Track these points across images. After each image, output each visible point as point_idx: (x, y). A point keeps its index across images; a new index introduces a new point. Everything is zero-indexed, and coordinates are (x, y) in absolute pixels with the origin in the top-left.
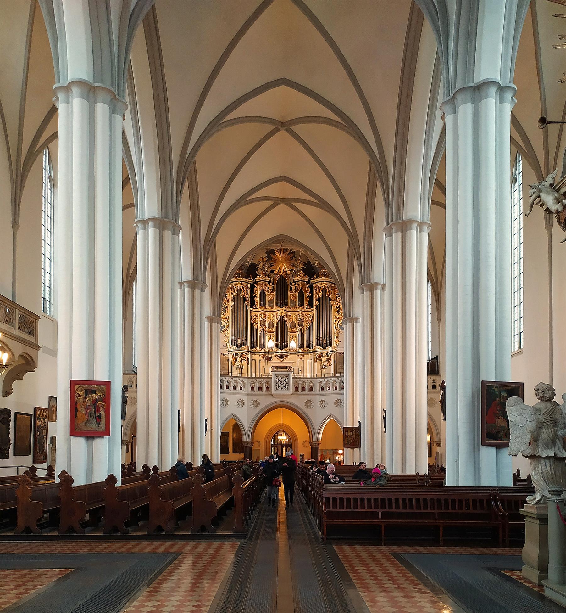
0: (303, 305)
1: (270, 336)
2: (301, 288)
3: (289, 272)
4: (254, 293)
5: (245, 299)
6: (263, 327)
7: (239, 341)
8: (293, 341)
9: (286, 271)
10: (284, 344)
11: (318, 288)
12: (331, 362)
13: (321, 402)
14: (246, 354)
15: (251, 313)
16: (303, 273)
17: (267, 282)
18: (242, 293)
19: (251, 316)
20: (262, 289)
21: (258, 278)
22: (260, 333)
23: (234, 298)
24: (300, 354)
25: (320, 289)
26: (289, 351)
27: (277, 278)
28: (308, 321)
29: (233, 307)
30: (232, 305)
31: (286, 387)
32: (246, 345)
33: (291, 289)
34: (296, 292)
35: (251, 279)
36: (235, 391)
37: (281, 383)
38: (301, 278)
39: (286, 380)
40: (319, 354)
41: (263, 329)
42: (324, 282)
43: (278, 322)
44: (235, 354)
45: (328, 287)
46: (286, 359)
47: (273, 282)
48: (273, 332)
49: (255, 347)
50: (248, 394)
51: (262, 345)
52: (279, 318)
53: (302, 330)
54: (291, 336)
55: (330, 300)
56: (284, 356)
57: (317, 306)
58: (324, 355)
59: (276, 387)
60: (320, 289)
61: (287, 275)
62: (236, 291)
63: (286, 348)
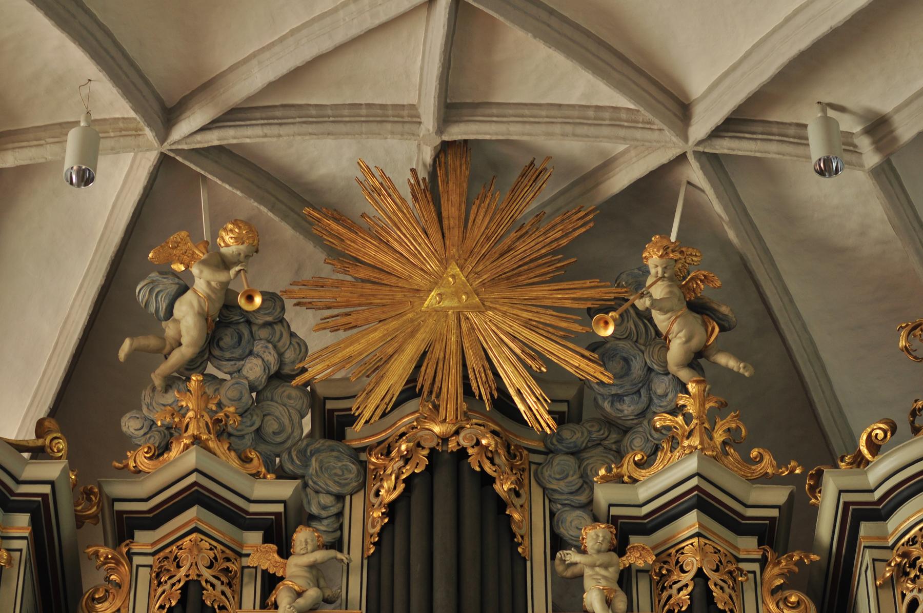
2: (700, 573)
16: (723, 407)
20: (191, 589)
38: (691, 465)
61: (511, 456)
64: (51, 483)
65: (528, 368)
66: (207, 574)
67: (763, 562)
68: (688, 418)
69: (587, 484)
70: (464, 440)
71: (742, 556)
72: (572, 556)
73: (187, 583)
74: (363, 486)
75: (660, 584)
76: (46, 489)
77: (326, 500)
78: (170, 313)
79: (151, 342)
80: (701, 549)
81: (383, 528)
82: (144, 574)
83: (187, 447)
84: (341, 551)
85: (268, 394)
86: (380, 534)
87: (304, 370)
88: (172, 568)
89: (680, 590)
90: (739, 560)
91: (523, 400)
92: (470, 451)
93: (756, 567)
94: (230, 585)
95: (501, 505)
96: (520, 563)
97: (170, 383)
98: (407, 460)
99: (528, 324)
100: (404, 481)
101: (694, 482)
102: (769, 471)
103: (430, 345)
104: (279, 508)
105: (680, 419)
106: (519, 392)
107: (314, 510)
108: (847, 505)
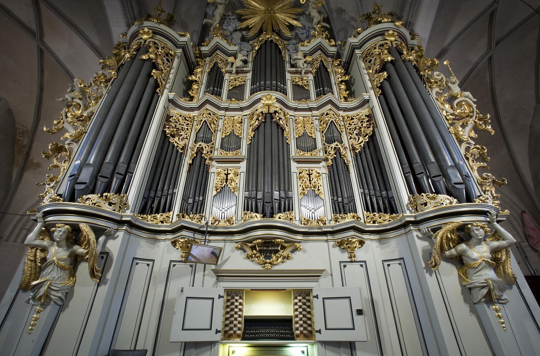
1: (227, 175)
2: (321, 60)
6: (204, 145)
15: (166, 108)
19: (167, 118)
20: (216, 64)
34: (306, 73)
41: (200, 151)
46: (288, 258)
48: (238, 161)
54: (305, 174)
63: (284, 211)
64: (186, 42)
77: (246, 52)
85: (233, 33)
102: (334, 44)
103: (265, 21)
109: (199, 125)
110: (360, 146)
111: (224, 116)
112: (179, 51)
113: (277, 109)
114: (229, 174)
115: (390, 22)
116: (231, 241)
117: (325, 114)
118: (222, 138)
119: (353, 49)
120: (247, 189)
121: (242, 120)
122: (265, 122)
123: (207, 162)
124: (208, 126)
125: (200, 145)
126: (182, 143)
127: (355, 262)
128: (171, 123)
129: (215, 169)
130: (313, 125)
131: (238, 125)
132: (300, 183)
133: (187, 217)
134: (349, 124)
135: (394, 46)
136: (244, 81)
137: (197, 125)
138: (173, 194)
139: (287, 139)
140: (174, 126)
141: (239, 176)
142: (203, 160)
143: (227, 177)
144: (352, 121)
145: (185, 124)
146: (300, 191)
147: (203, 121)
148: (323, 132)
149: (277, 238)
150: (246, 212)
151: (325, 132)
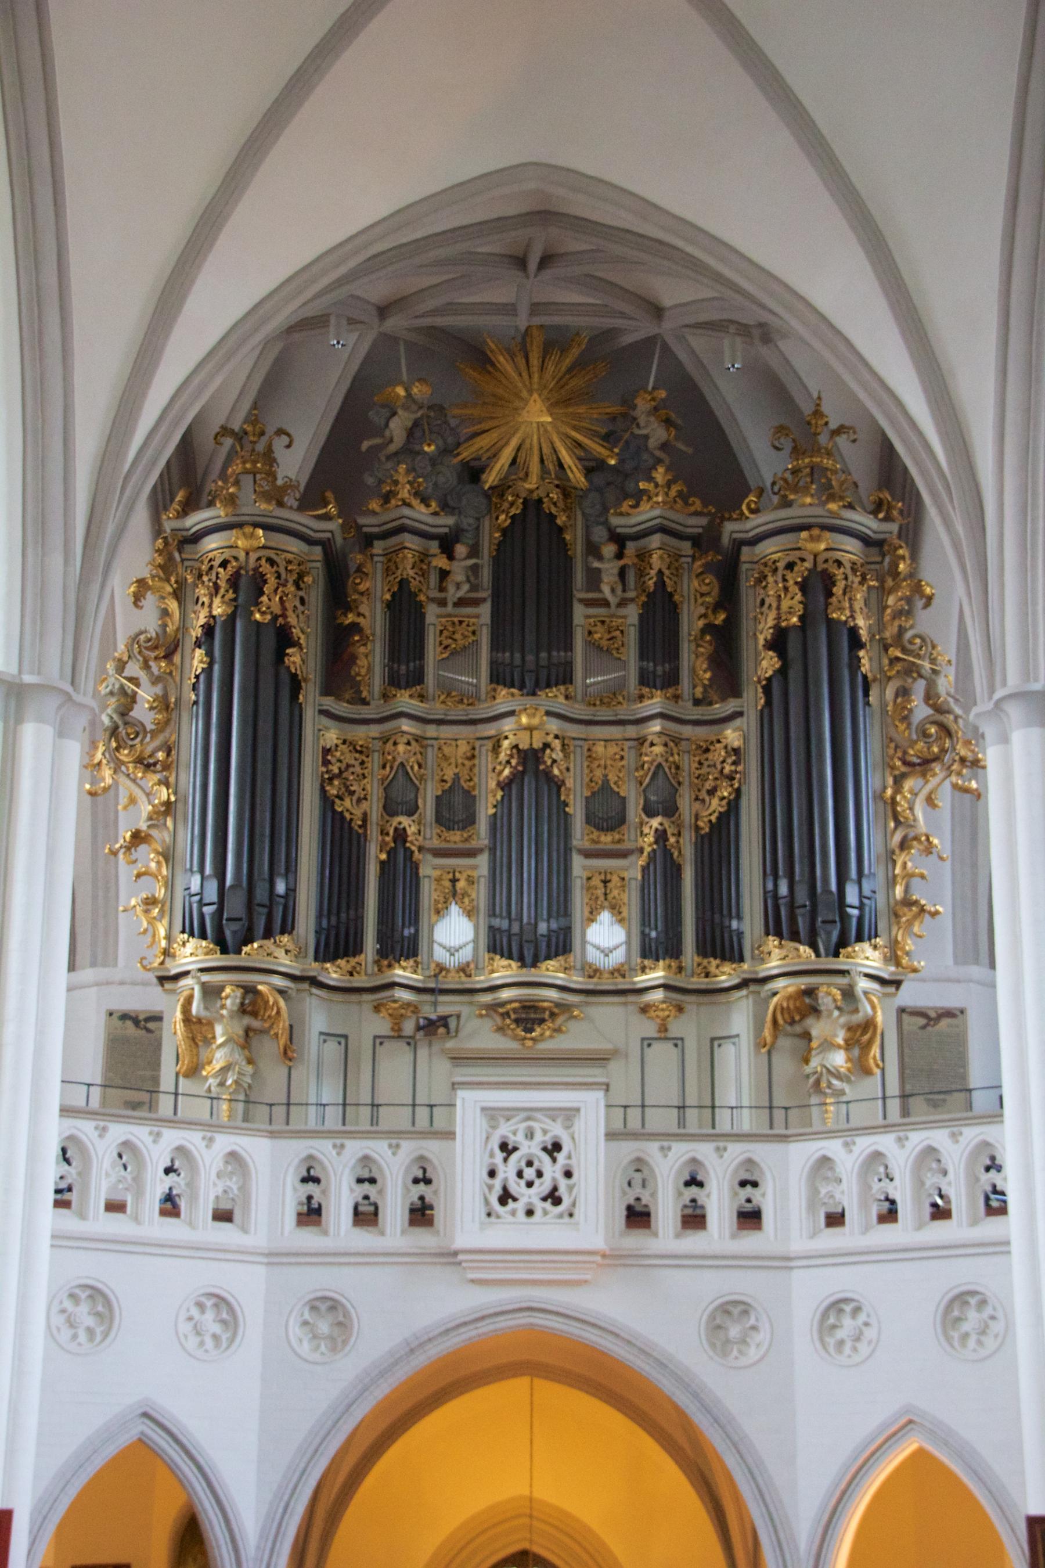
0: (671, 680)
1: (454, 881)
2: (660, 572)
3: (577, 476)
4: (348, 608)
5: (284, 638)
6: (405, 821)
7: (236, 906)
8: (605, 916)
9: (561, 465)
10: (543, 928)
11: (776, 570)
12: (875, 1050)
13: (825, 1315)
14: (281, 992)
17: (434, 547)
18: (264, 599)
21: (374, 513)
22: (384, 856)
23: (209, 630)
24: (658, 995)
25: (789, 576)
26: (577, 980)
27: (502, 517)
28: (709, 785)
29: (202, 686)
30: (197, 677)
31: (557, 1201)
32: (282, 933)
33: (594, 579)
34: (623, 603)
35: (327, 517)
36: (171, 1229)
37: (520, 1174)
38: (657, 512)
39: (557, 1147)
40: (791, 989)
41: (401, 835)
42: (816, 532)
43: (505, 786)
44: (204, 986)
45: (839, 563)
46: (558, 1030)
47: (477, 536)
48: (472, 853)
49: (346, 955)
50: (275, 1258)
51: (397, 935)
52: (514, 762)
53: (667, 840)
54: (596, 881)
55: (855, 642)
56: (544, 1009)
57: (769, 680)
58: (825, 1001)
59: (487, 1202)
60: (789, 576)
62: (222, 583)
63: (557, 955)
64: (331, 532)
65: (575, 454)
66: (411, 573)
67: (694, 557)
68: (657, 485)
69: (605, 510)
70: (541, 493)
71: (684, 553)
72: (596, 564)
73: (402, 579)
74: (489, 511)
75: (641, 574)
76: (329, 535)
77: (471, 521)
78: (387, 425)
79: (378, 441)
80: (661, 558)
81: (500, 542)
82: (379, 565)
83: (397, 506)
84: (477, 557)
86: (499, 545)
87: (458, 454)
88: (394, 568)
89: (650, 579)
90: (682, 556)
91: (572, 471)
92: (545, 500)
93: (689, 560)
94: (423, 575)
95: (561, 530)
96: (569, 560)
97: (388, 458)
98: (512, 504)
99: (575, 428)
100: (513, 517)
101: (658, 521)
103: (523, 441)
104: (446, 530)
105: (652, 484)
106: (570, 468)
107: (466, 527)
108: (735, 540)
109: (388, 769)
110: (710, 821)
111: (436, 739)
112: (318, 551)
113: (550, 739)
114: (458, 880)
115: (817, 505)
116: (471, 1003)
117: (648, 742)
118: (437, 797)
119: (739, 544)
120: (492, 914)
121: (474, 749)
122: (523, 773)
123: (417, 856)
124: (407, 773)
125: (400, 823)
126: (358, 812)
127: (667, 1039)
128: (330, 767)
129: (429, 868)
130: (623, 763)
131: (466, 762)
132: (586, 900)
133: (397, 965)
134: (700, 763)
135: (821, 567)
136: (474, 633)
137: (384, 767)
138: (359, 920)
139: (566, 805)
140: (336, 771)
141: (476, 886)
142: (408, 853)
143: (454, 886)
144: (706, 756)
145: (357, 763)
146: (587, 914)
147: (397, 763)
148: (641, 784)
149: (544, 1001)
150: (492, 955)
151: (644, 785)
